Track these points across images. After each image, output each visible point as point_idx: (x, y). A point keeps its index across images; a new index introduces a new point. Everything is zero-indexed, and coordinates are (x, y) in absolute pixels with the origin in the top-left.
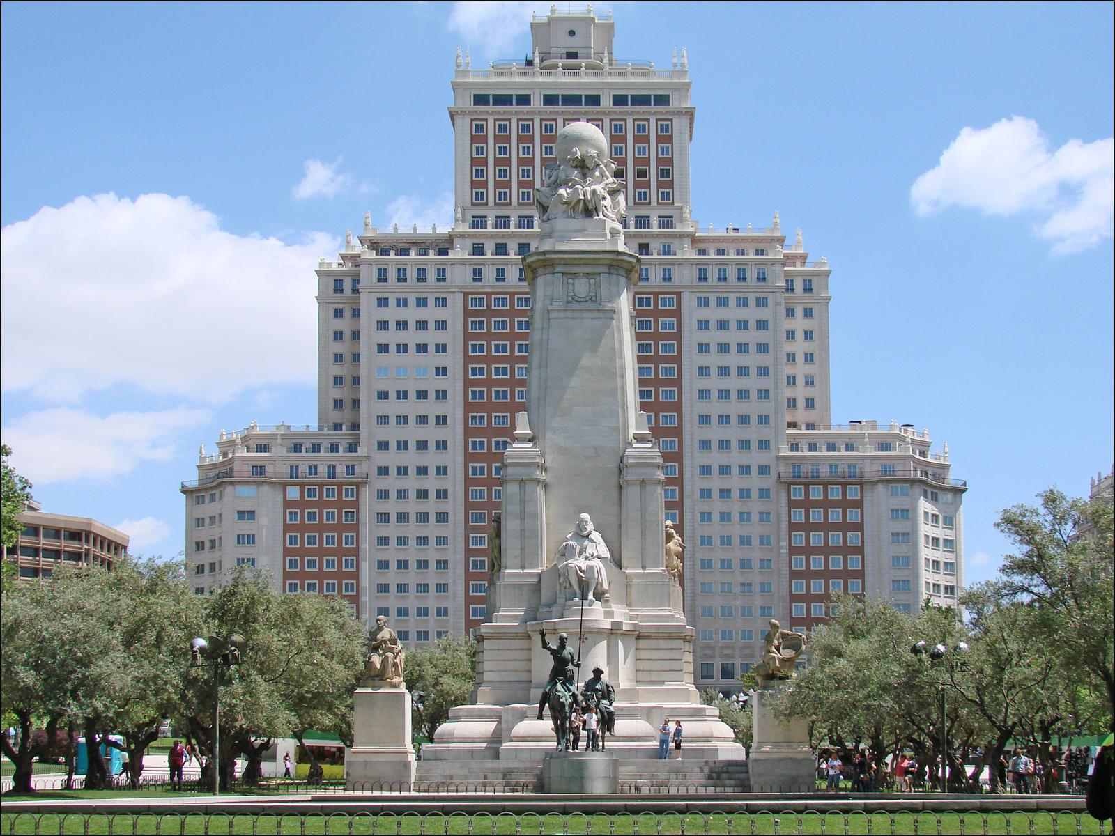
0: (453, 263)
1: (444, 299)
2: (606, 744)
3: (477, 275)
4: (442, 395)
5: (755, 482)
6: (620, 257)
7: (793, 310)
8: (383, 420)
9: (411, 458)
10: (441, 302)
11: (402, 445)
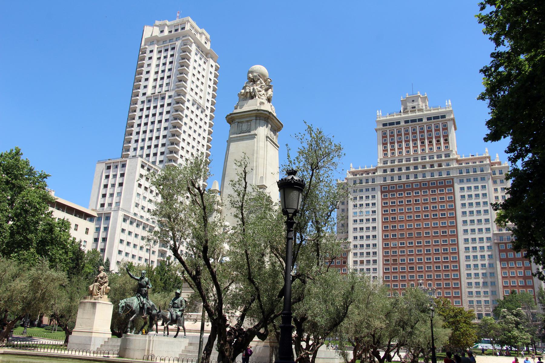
0: (377, 176)
1: (374, 188)
2: (186, 333)
3: (385, 179)
4: (374, 220)
5: (486, 244)
6: (259, 112)
7: (496, 181)
8: (355, 229)
9: (365, 242)
10: (373, 189)
11: (362, 237)
